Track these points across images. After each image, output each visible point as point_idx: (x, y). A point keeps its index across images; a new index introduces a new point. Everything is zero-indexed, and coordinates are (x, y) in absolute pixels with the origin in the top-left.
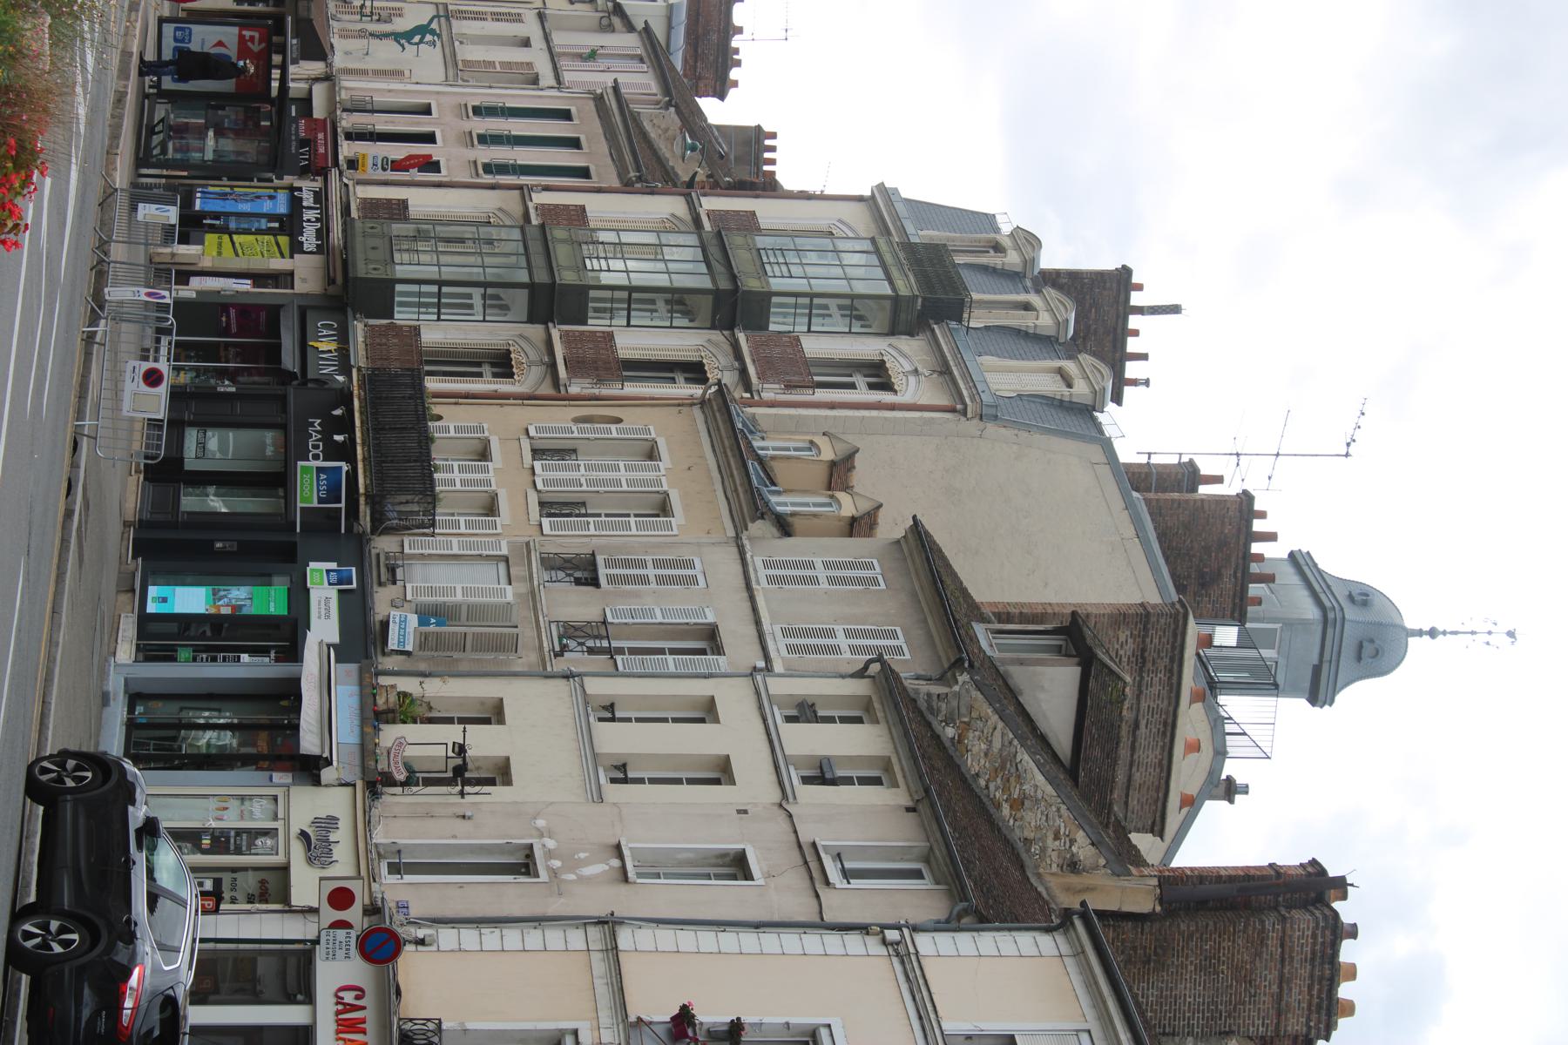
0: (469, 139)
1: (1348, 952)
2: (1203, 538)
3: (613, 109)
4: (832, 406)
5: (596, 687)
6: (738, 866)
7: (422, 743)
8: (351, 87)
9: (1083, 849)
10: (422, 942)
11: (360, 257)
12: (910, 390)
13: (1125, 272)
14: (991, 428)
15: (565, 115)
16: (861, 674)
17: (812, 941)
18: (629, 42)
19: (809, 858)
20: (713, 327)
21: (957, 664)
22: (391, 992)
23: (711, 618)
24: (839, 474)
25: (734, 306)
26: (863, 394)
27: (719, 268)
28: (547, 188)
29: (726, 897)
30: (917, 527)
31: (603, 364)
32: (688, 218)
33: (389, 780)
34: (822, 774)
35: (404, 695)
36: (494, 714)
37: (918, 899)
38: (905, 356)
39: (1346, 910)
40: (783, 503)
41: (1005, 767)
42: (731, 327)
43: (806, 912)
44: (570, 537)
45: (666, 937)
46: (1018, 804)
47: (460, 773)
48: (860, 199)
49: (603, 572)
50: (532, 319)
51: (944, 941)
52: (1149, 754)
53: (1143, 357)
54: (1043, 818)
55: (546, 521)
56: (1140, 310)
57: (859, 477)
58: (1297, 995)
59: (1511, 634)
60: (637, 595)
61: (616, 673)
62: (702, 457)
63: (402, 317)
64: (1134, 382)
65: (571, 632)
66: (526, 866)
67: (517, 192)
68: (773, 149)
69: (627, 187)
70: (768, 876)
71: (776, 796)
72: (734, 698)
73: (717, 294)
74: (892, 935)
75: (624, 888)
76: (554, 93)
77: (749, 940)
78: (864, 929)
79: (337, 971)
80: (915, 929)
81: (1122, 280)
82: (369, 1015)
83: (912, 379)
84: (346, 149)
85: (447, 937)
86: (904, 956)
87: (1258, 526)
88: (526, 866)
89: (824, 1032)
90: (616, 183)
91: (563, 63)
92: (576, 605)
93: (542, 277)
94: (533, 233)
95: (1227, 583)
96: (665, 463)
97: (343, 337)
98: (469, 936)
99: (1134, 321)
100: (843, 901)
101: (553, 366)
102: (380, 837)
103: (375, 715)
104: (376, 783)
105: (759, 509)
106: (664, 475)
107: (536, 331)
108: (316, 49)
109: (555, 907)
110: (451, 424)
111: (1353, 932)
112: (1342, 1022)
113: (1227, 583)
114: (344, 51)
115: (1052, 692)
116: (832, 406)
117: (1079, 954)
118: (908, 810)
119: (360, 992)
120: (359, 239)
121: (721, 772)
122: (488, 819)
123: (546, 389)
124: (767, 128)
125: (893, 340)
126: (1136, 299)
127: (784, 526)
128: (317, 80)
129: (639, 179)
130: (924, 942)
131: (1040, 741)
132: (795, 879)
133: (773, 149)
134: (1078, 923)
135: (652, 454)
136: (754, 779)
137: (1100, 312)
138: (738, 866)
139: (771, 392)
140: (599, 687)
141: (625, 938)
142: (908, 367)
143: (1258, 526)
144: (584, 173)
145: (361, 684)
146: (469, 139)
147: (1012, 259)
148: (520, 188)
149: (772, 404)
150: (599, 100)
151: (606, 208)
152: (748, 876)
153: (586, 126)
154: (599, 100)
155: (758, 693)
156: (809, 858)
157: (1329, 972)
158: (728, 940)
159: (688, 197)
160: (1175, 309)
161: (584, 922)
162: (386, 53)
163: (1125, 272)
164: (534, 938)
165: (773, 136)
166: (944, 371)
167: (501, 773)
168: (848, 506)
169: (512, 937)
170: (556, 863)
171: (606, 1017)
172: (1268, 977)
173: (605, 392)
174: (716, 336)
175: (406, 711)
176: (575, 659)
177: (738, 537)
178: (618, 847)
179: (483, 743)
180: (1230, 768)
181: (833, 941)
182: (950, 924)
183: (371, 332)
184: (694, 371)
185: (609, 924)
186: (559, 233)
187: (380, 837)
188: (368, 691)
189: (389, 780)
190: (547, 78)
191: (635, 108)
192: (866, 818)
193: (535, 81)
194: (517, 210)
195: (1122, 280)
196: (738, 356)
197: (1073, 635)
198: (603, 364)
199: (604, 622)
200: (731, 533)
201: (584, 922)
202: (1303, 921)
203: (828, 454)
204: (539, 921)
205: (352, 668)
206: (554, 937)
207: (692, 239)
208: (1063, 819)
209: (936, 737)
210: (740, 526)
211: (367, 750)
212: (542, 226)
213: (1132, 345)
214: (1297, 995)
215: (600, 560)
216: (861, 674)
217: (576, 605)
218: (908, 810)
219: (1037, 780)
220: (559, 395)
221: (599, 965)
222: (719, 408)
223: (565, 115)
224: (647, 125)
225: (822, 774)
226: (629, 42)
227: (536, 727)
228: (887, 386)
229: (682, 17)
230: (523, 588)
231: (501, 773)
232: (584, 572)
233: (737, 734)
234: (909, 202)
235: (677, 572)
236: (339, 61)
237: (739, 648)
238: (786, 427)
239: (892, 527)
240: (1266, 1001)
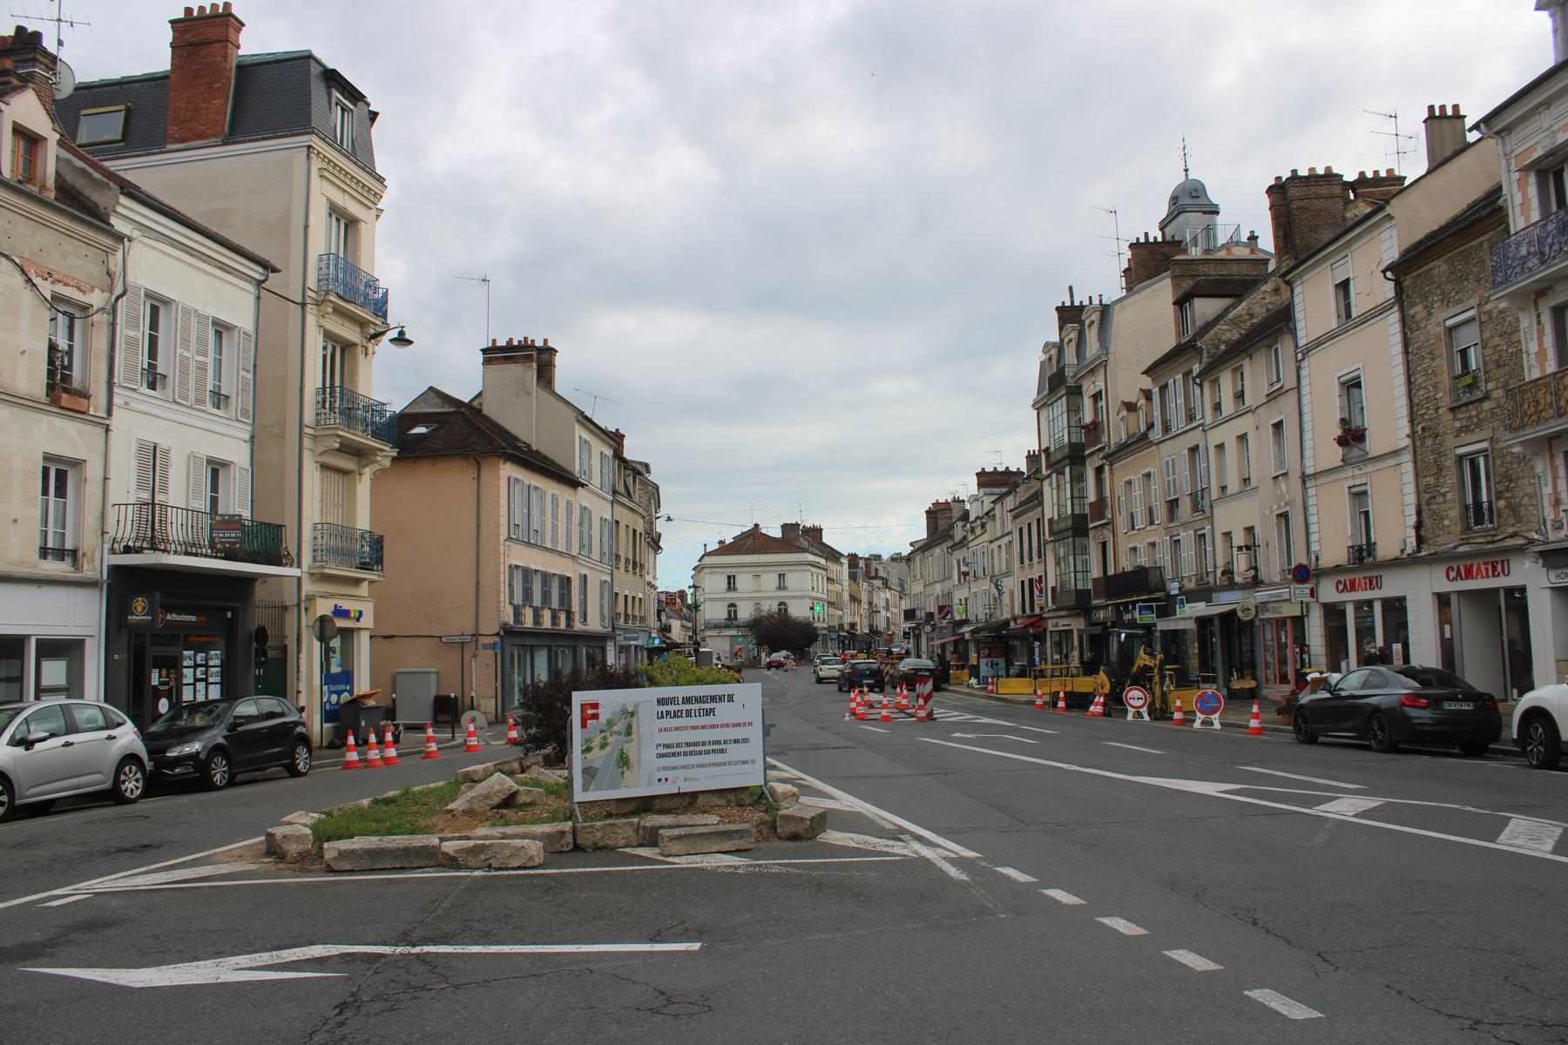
0: (1031, 566)
1: (1303, 172)
2: (1149, 260)
5: (1214, 495)
6: (1278, 426)
7: (1241, 563)
8: (1017, 611)
12: (1100, 384)
13: (1058, 309)
14: (1111, 350)
16: (1201, 385)
17: (1305, 391)
18: (998, 507)
19: (1273, 397)
21: (1194, 347)
22: (1337, 569)
24: (1131, 407)
25: (1075, 456)
26: (1103, 403)
29: (1290, 430)
30: (1148, 372)
31: (1100, 506)
33: (1256, 576)
34: (1240, 396)
35: (1223, 573)
36: (1228, 535)
37: (1285, 348)
38: (1089, 388)
39: (1286, 175)
40: (1143, 428)
41: (1235, 323)
43: (1294, 394)
44: (1161, 514)
45: (1308, 453)
46: (1251, 316)
47: (1250, 547)
50: (1087, 535)
51: (1300, 334)
52: (1235, 269)
54: (1257, 304)
57: (1133, 400)
58: (1324, 191)
61: (1209, 488)
63: (1090, 586)
65: (1196, 507)
66: (1284, 516)
69: (1041, 504)
72: (1215, 437)
73: (1071, 464)
74: (1300, 356)
77: (1307, 418)
78: (1298, 369)
79: (1329, 592)
81: (1061, 310)
82: (1347, 577)
84: (1037, 611)
85: (1315, 547)
86: (1307, 351)
87: (1142, 240)
88: (1284, 516)
92: (1185, 507)
95: (1167, 250)
96: (1132, 477)
97: (1098, 608)
98: (1314, 538)
100: (1289, 381)
102: (1277, 579)
103: (1231, 585)
104: (1256, 582)
105: (1145, 436)
106: (1136, 478)
107: (1091, 533)
108: (1007, 623)
109: (1299, 502)
110: (1126, 564)
111: (1294, 171)
112: (1335, 171)
113: (1167, 250)
114: (1007, 615)
115: (1205, 308)
117: (1300, 275)
119: (1339, 582)
121: (1242, 438)
122: (1268, 533)
126: (1068, 304)
127: (1151, 426)
130: (1301, 342)
131: (1227, 311)
132: (1281, 401)
135: (1129, 483)
136: (1244, 424)
137: (1069, 315)
138: (1278, 426)
140: (1215, 494)
141: (1310, 471)
143: (1142, 240)
146: (1031, 566)
147: (1054, 352)
150: (1015, 517)
151: (1050, 511)
152: (1281, 422)
153: (1023, 521)
154: (1015, 517)
156: (1273, 397)
157: (1313, 178)
158: (1307, 426)
161: (1305, 489)
162: (1006, 599)
163: (1058, 309)
164: (1312, 510)
166: (1092, 371)
167: (1250, 530)
168: (1142, 402)
169: (1313, 519)
171: (1342, 476)
172: (1318, 204)
175: (1228, 572)
176: (1206, 503)
178: (1275, 478)
179: (1239, 539)
180: (1244, 239)
181: (1304, 382)
182: (1293, 332)
183: (1097, 597)
184: (1099, 471)
185: (1304, 478)
187: (1277, 579)
189: (1256, 576)
192: (1256, 375)
197: (1181, 302)
198: (1100, 506)
201: (1305, 489)
202: (1293, 192)
203: (1124, 413)
204: (1305, 509)
206: (1312, 501)
208: (1256, 296)
209: (1225, 352)
210: (1151, 444)
211: (1243, 587)
214: (1324, 191)
216: (1201, 385)
217: (1185, 507)
219: (1241, 308)
220: (1112, 522)
221: (1321, 481)
222: (1113, 457)
225: (1240, 396)
226: (998, 507)
227: (1231, 518)
229: (988, 490)
231: (1250, 530)
232: (1173, 505)
233: (1226, 434)
235: (1170, 467)
237: (1195, 438)
238: (1116, 432)
239: (1147, 382)
240: (1329, 203)
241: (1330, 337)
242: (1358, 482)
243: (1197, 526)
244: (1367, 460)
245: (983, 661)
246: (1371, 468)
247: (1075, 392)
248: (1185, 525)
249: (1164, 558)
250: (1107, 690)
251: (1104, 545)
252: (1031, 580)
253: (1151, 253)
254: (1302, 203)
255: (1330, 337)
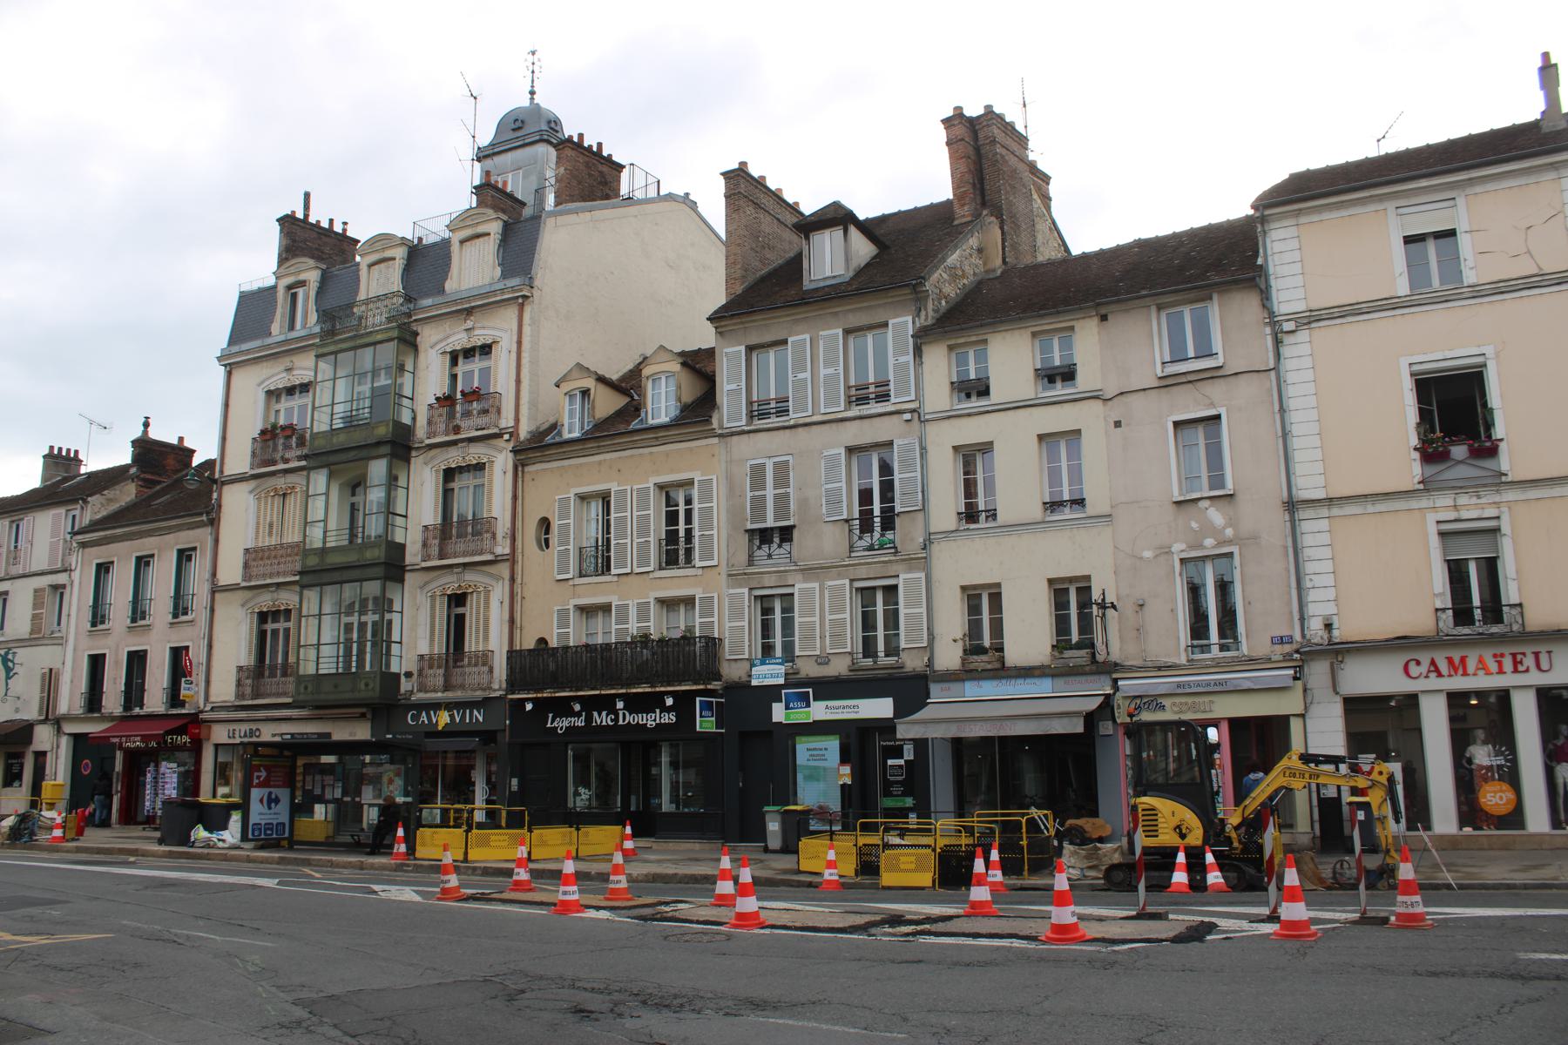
3: (85, 535)
4: (518, 381)
9: (973, 242)
10: (1328, 627)
11: (347, 696)
14: (537, 283)
15: (103, 569)
19: (1168, 383)
20: (408, 461)
23: (843, 451)
27: (374, 452)
28: (214, 574)
32: (253, 484)
38: (436, 341)
42: (410, 449)
48: (229, 374)
49: (770, 522)
50: (402, 581)
53: (331, 221)
55: (614, 571)
56: (306, 216)
59: (533, 53)
60: (804, 503)
62: (600, 463)
64: (345, 230)
67: (217, 595)
68: (69, 451)
69: (214, 522)
70: (1212, 405)
71: (1099, 403)
75: (1240, 497)
76: (76, 575)
78: (1278, 343)
80: (1271, 314)
83: (477, 332)
85: (1318, 609)
89: (1416, 368)
90: (209, 529)
91: (15, 571)
92: (823, 539)
93: (379, 571)
94: (307, 579)
95: (605, 169)
96: (614, 487)
97: (436, 706)
99: (312, 220)
101: (465, 565)
102: (1183, 660)
103: (1002, 671)
113: (605, 169)
116: (518, 381)
118: (1104, 318)
120: (323, 697)
123: (504, 570)
124: (47, 451)
125: (421, 348)
126: (300, 215)
128: (59, 731)
129: (208, 513)
133: (69, 451)
134: (1267, 212)
139: (507, 421)
142: (464, 335)
144: (185, 556)
145: (963, 680)
148: (213, 592)
149: (517, 420)
154: (83, 545)
155: (949, 417)
156: (1168, 383)
159: (224, 483)
160: (307, 196)
165: (52, 448)
166: (469, 312)
170: (1209, 542)
173: (503, 526)
174: (417, 462)
177: (720, 436)
178: (1178, 503)
183: (422, 689)
185: (1292, 506)
186: (313, 561)
188: (966, 674)
190: (61, 579)
191: (86, 521)
193: (58, 589)
194: (240, 596)
195: (288, 222)
196: (454, 443)
199: (847, 521)
200: (715, 440)
203: (589, 383)
205: (935, 689)
207: (313, 475)
210: (712, 434)
212: (300, 573)
213: (325, 225)
215: (750, 526)
218: (1104, 318)
220: (512, 559)
223: (103, 569)
224: (99, 516)
228: (486, 350)
230: (799, 576)
234: (233, 340)
236: (31, 713)
241: (1391, 305)
242: (1465, 514)
243: (862, 572)
244: (1499, 481)
245: (256, 793)
246: (1510, 495)
247: (408, 340)
248: (809, 572)
249: (730, 622)
250: (1196, 837)
251: (458, 599)
252: (137, 660)
253: (587, 165)
254: (1004, 152)
255: (1391, 305)
